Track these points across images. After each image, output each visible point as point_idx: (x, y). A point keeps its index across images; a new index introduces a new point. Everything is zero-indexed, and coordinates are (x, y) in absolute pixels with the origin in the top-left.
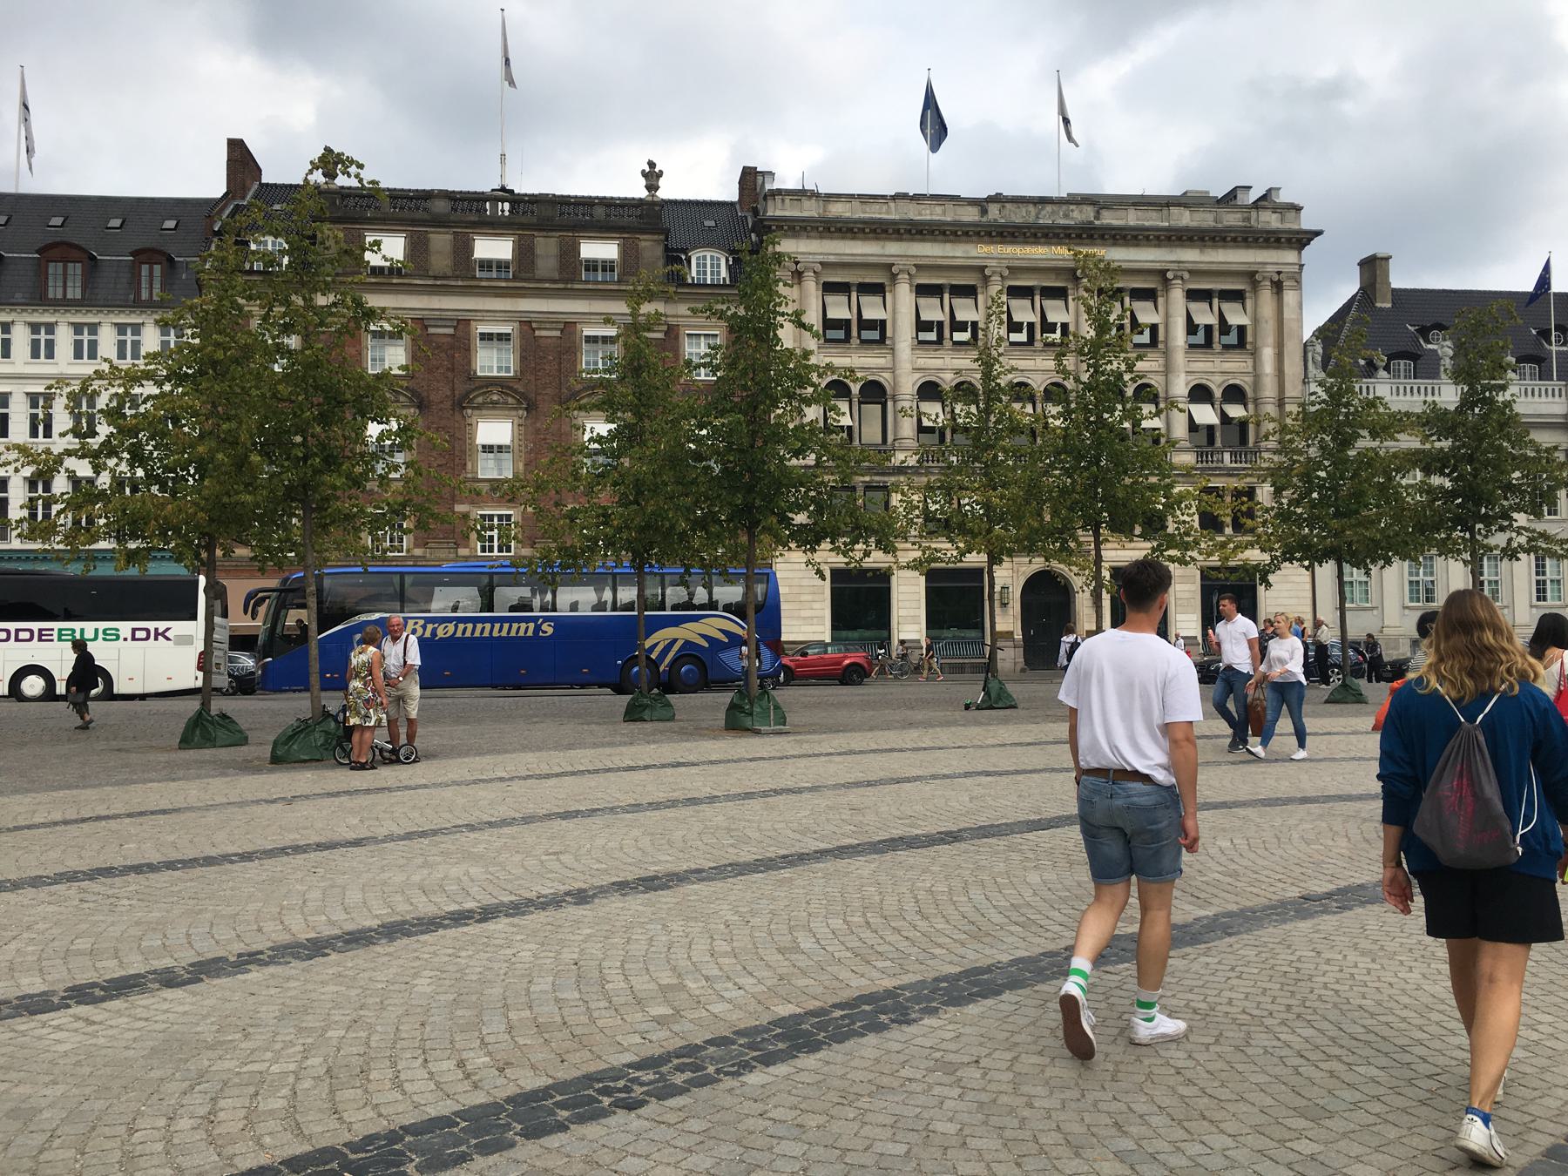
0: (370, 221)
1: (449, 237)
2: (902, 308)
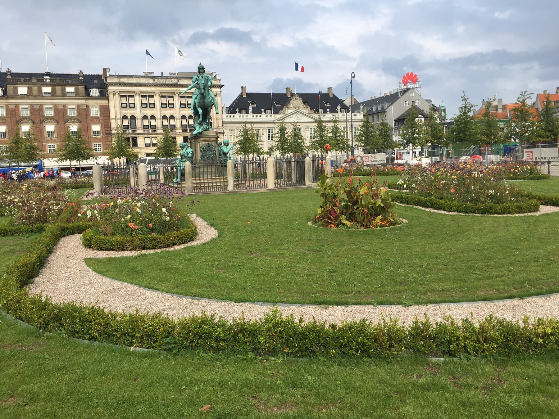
0: (19, 84)
1: (37, 87)
2: (137, 100)
